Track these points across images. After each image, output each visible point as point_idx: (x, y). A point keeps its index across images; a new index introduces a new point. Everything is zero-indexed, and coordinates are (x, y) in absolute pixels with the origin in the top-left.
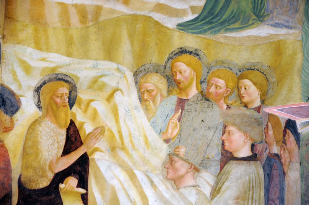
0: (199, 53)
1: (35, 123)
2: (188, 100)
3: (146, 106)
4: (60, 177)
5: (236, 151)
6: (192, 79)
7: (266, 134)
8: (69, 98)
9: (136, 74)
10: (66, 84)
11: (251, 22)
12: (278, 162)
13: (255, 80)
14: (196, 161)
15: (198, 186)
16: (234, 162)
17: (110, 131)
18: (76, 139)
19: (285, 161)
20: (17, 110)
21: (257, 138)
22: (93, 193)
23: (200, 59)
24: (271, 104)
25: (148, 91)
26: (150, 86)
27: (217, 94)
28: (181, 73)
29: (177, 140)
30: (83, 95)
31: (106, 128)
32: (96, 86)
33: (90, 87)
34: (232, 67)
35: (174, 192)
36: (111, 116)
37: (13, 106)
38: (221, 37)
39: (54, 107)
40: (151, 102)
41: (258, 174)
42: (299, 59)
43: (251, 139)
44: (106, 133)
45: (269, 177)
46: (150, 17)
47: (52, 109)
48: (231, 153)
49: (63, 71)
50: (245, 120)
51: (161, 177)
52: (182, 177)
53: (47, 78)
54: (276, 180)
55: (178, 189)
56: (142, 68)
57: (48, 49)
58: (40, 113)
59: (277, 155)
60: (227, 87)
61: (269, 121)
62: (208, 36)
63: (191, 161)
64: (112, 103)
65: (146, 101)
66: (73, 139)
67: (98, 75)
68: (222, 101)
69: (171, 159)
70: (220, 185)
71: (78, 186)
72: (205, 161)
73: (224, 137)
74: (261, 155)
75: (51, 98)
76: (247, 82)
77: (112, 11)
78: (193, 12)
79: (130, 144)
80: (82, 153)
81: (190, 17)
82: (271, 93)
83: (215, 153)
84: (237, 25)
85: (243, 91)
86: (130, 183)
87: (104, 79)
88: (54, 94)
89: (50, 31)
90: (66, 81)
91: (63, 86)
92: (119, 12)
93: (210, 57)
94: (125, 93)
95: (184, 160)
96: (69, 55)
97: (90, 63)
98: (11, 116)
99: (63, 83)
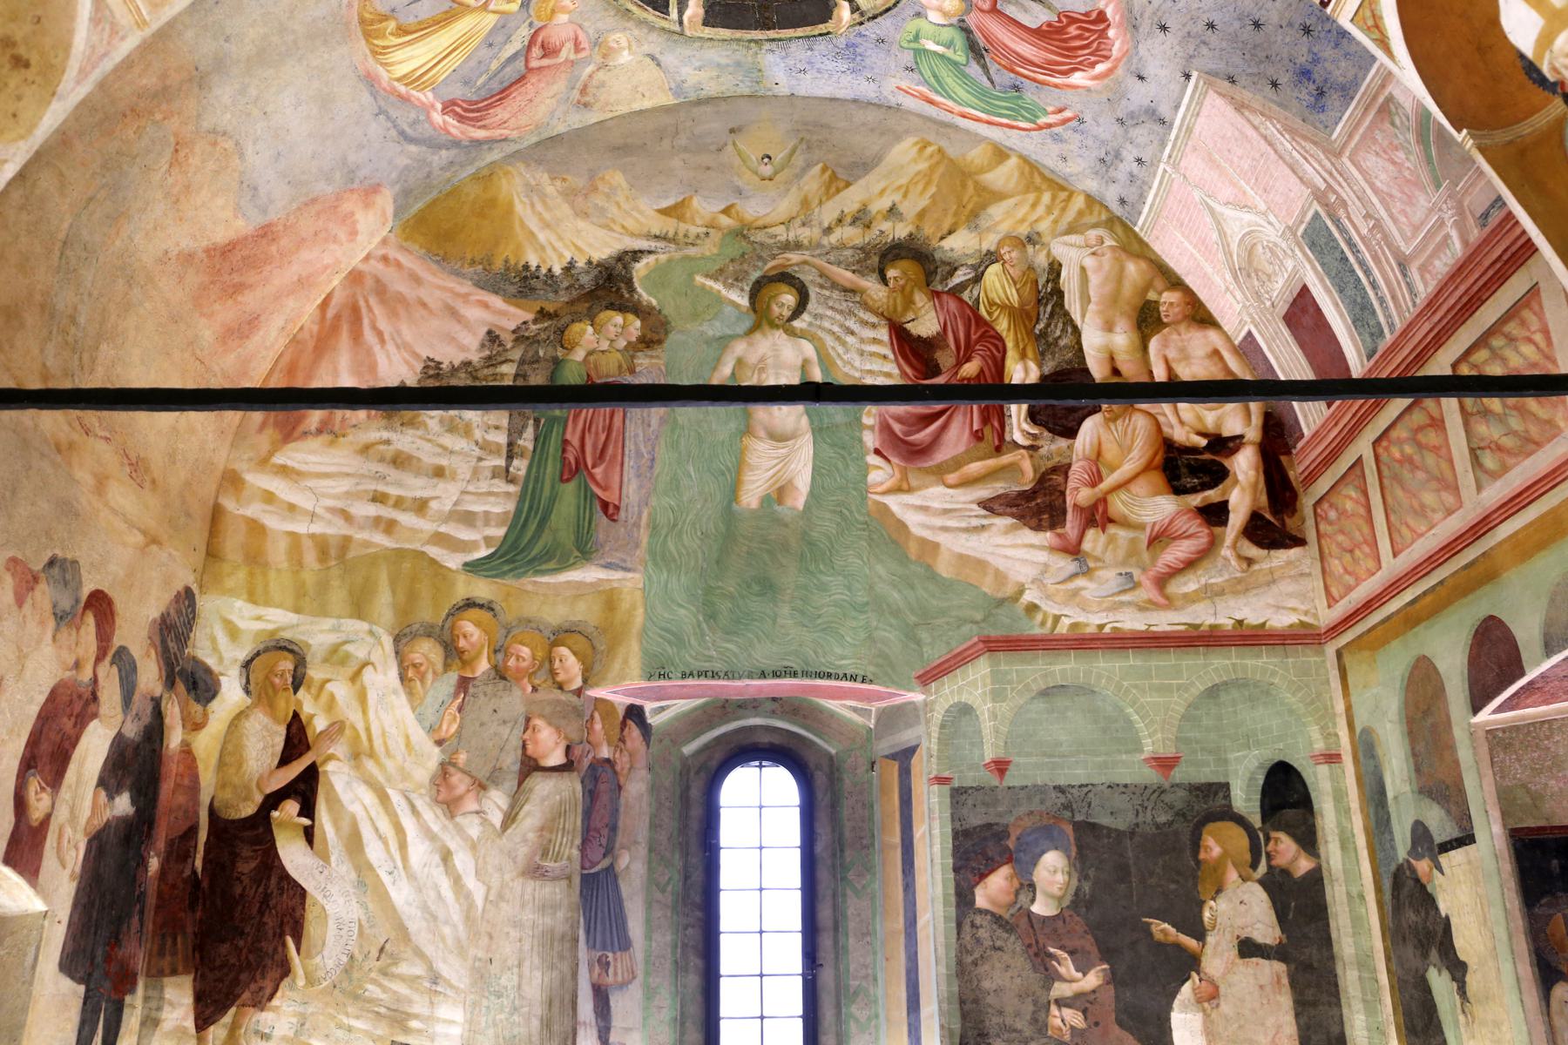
0: (494, 606)
1: (240, 716)
2: (474, 678)
3: (410, 688)
4: (274, 800)
5: (545, 756)
6: (483, 646)
7: (590, 729)
8: (294, 677)
9: (397, 640)
10: (290, 656)
11: (572, 561)
12: (609, 770)
13: (575, 648)
14: (482, 774)
15: (484, 812)
16: (540, 774)
17: (354, 728)
18: (300, 741)
19: (623, 769)
20: (214, 696)
21: (575, 736)
22: (322, 826)
23: (495, 616)
24: (597, 685)
25: (414, 665)
26: (417, 657)
27: (518, 669)
28: (465, 637)
29: (455, 741)
30: (315, 673)
31: (348, 723)
32: (335, 658)
33: (325, 660)
34: (542, 627)
35: (447, 822)
36: (355, 704)
37: (208, 690)
38: (529, 582)
39: (270, 691)
40: (418, 683)
41: (574, 793)
42: (639, 617)
43: (566, 738)
44: (347, 732)
45: (591, 795)
46: (423, 553)
47: (267, 694)
48: (535, 760)
49: (287, 635)
50: (558, 709)
51: (427, 799)
52: (460, 798)
53: (261, 647)
54: (604, 798)
55: (452, 816)
56: (408, 630)
57: (268, 603)
58: (249, 701)
59: (608, 761)
60: (534, 659)
61: (596, 709)
62: (509, 581)
63: (474, 773)
64: (358, 683)
65: (411, 680)
66: (296, 741)
67: (339, 640)
68: (526, 680)
69: (445, 770)
70: (517, 809)
71: (300, 815)
72: (497, 774)
73: (526, 736)
74: (579, 762)
75: (267, 677)
76: (564, 651)
77: (367, 544)
78: (488, 547)
79: (383, 749)
80: (309, 763)
81: (483, 552)
82: (597, 667)
83: (511, 761)
84: (551, 565)
85: (557, 664)
86: (381, 809)
87: (349, 648)
88: (271, 671)
89: (272, 575)
90: (291, 651)
91: (285, 659)
92: (377, 545)
93: (509, 616)
94: (379, 668)
95: (464, 772)
96: (297, 610)
97: (328, 623)
98: (205, 706)
99: (286, 653)
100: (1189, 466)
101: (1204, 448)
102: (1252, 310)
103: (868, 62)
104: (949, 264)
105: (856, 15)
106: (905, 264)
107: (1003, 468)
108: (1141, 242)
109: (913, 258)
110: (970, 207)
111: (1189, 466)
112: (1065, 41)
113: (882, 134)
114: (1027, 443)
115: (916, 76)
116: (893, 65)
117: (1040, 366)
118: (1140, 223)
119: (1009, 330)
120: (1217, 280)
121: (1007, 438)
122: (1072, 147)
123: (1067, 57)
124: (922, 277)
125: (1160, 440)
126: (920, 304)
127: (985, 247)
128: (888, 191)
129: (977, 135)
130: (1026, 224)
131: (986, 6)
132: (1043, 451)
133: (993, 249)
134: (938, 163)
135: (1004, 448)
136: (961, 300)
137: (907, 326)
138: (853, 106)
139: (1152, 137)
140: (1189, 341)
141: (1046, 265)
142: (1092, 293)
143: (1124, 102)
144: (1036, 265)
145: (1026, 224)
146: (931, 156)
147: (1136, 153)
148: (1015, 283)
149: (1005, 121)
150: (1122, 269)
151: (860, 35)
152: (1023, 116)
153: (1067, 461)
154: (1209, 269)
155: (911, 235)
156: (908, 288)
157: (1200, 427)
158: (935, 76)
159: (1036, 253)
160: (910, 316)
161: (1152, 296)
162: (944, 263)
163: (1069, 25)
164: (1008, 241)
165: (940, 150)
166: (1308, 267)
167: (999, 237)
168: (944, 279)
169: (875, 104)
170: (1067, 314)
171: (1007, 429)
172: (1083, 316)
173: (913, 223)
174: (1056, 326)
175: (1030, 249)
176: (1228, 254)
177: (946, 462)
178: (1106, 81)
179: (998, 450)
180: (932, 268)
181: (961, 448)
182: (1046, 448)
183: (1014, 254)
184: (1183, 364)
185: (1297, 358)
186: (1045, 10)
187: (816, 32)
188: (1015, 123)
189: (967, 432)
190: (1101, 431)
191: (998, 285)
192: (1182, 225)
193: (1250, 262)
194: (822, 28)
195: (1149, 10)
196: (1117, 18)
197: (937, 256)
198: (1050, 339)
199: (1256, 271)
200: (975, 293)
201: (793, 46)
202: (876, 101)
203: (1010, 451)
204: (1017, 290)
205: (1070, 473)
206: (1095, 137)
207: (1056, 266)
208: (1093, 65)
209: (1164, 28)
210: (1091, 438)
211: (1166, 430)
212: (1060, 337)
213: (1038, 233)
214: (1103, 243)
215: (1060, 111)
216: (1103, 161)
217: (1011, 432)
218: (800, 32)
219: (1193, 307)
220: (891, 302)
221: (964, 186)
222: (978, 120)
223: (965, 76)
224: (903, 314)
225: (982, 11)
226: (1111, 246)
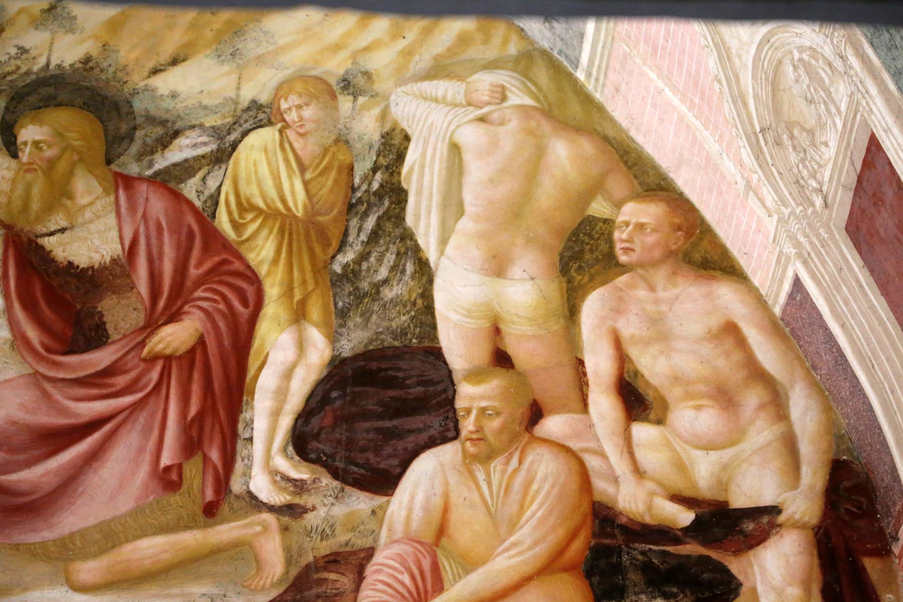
100: (647, 568)
101: (686, 530)
102: (794, 226)
104: (163, 123)
106: (63, 117)
107: (215, 553)
108: (587, 100)
109: (85, 106)
111: (647, 568)
114: (278, 498)
117: (333, 338)
118: (584, 59)
119: (275, 262)
120: (729, 166)
121: (236, 485)
124: (99, 146)
125: (586, 507)
126: (83, 200)
127: (248, 94)
132: (312, 519)
133: (264, 98)
135: (225, 508)
136: (178, 197)
137: (48, 243)
140: (671, 303)
141: (376, 137)
142: (468, 197)
144: (353, 136)
145: (343, 55)
148: (303, 169)
150: (540, 152)
153: (367, 542)
154: (713, 147)
155: (87, 60)
156: (62, 167)
157: (680, 485)
159: (356, 112)
160: (58, 220)
161: (599, 208)
162: (151, 120)
164: (299, 86)
166: (873, 90)
167: (281, 76)
168: (148, 152)
170: (407, 236)
171: (239, 466)
172: (444, 241)
173: (96, 37)
174: (380, 260)
175: (345, 103)
176: (739, 99)
177: (83, 533)
179: (211, 511)
180: (124, 127)
181: (125, 504)
182: (322, 512)
183: (307, 113)
184: (654, 349)
185: (879, 319)
189: (144, 470)
190: (453, 479)
191: (264, 170)
192: (655, 49)
193: (777, 110)
197: (139, 105)
198: (365, 285)
199: (789, 127)
200: (212, 184)
203: (236, 515)
204: (306, 184)
205: (369, 569)
207: (396, 141)
210: (428, 501)
211: (601, 486)
212: (386, 281)
213: (367, 75)
214: (504, 98)
217: (247, 475)
219: (689, 234)
220: (20, 190)
224: (38, 220)
226: (522, 108)
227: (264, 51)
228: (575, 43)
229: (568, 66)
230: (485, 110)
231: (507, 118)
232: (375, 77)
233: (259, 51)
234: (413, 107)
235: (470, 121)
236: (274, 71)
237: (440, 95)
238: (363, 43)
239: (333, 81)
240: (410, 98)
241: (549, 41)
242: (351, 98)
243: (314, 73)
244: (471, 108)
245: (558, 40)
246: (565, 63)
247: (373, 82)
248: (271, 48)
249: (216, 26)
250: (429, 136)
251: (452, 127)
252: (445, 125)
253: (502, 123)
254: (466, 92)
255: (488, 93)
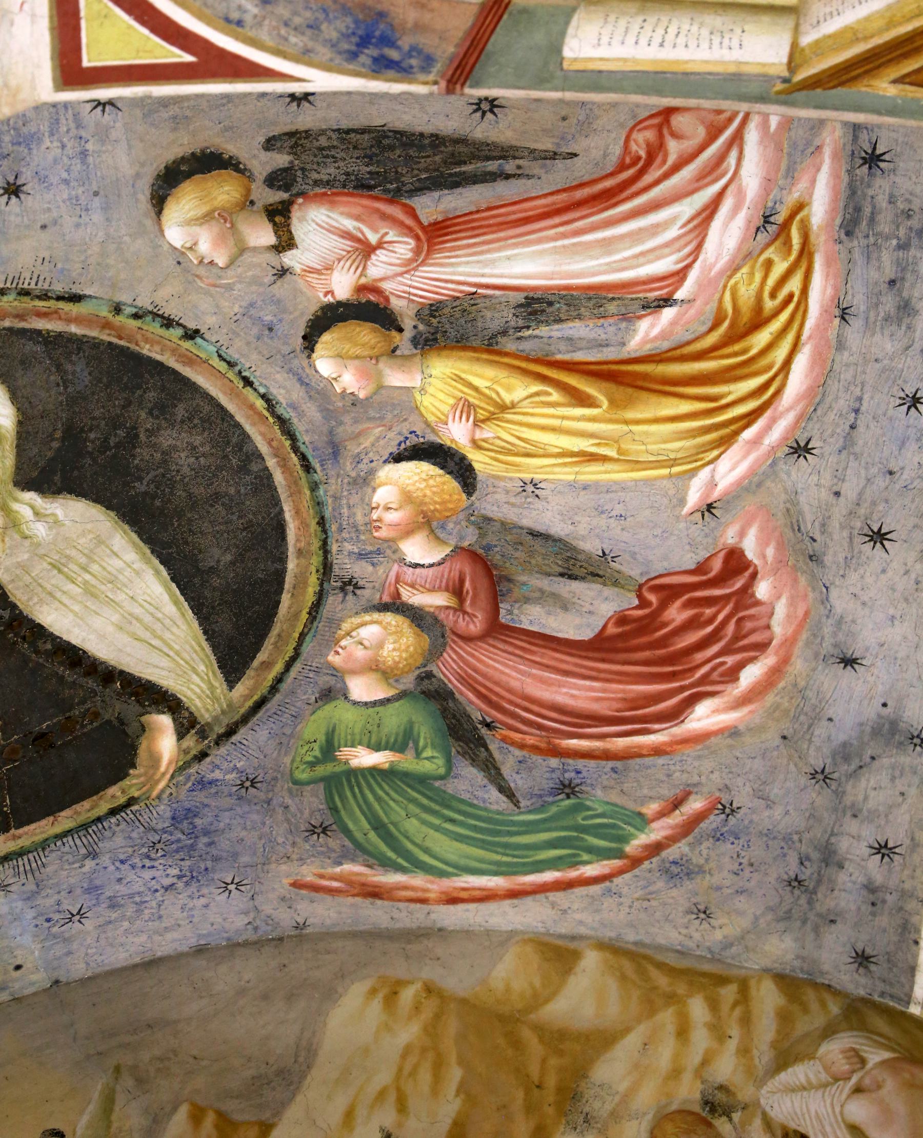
103: (224, 844)
105: (190, 741)
110: (551, 1081)
112: (663, 642)
113: (290, 998)
115: (335, 842)
116: (280, 834)
122: (716, 880)
123: (672, 676)
128: (361, 1112)
129: (488, 933)
130: (687, 1077)
131: (476, 626)
134: (437, 1017)
138: (200, 963)
139: (900, 785)
143: (821, 730)
145: (687, 1077)
146: (417, 1008)
147: (869, 834)
149: (549, 876)
151: (202, 784)
152: (590, 850)
158: (379, 827)
163: (664, 605)
165: (429, 989)
169: (246, 944)
178: (770, 699)
186: (608, 591)
187: (103, 808)
188: (573, 874)
194: (115, 794)
195: (839, 511)
196: (770, 552)
201: (52, 859)
202: (250, 935)
206: (768, 835)
208: (733, 674)
209: (879, 537)
213: (721, 1088)
214: (863, 1061)
215: (677, 804)
216: (796, 882)
218: (66, 820)
221: (517, 1044)
222: (487, 896)
223: (446, 801)
225: (468, 639)
226: (884, 1063)
227: (613, 1105)
228: (903, 979)
229: (896, 1006)
230: (855, 1079)
231: (880, 1079)
232: (732, 1088)
233: (608, 1107)
234: (789, 1104)
235: (848, 1097)
236: (635, 1123)
237: (803, 1080)
238: (696, 1058)
239: (697, 1108)
240: (779, 1095)
241: (865, 987)
242: (724, 1118)
243: (674, 1107)
244: (841, 1083)
245: (877, 982)
246: (891, 1004)
247: (734, 1094)
248: (617, 1099)
249: (551, 1099)
250: (823, 1127)
251: (837, 1110)
252: (830, 1110)
253: (879, 1087)
254: (826, 1069)
255: (844, 1061)
